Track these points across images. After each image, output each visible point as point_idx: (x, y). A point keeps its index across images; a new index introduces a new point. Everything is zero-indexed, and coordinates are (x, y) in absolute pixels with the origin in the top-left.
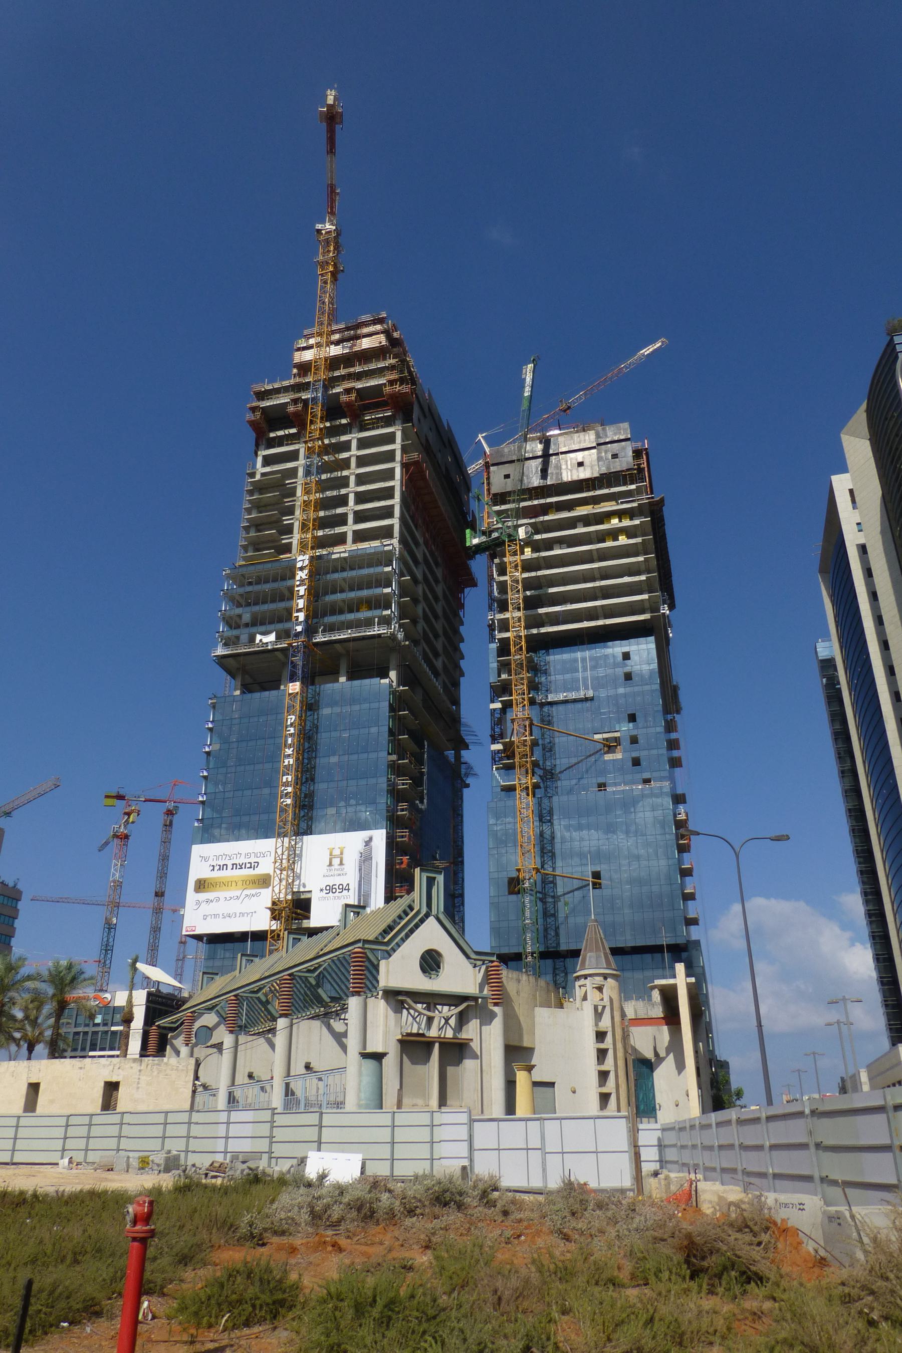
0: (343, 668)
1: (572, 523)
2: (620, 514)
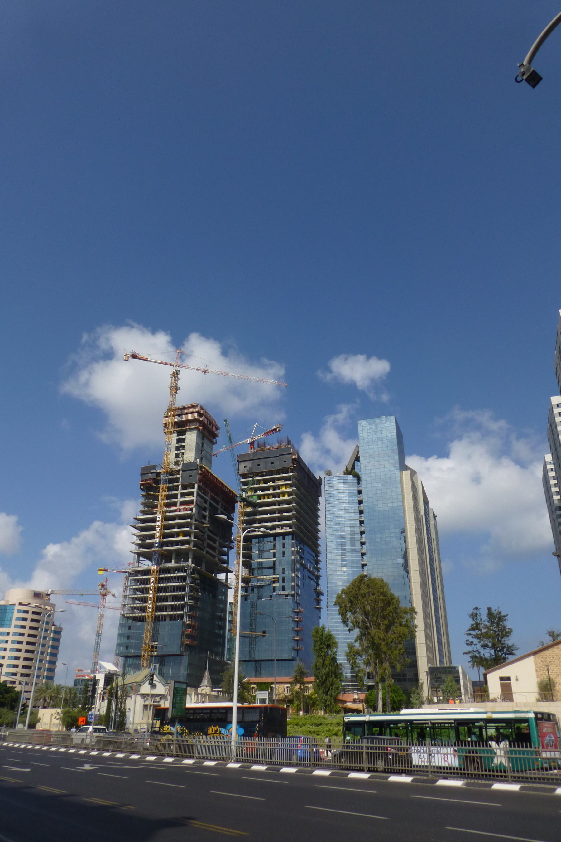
0: (173, 556)
1: (268, 489)
2: (286, 485)
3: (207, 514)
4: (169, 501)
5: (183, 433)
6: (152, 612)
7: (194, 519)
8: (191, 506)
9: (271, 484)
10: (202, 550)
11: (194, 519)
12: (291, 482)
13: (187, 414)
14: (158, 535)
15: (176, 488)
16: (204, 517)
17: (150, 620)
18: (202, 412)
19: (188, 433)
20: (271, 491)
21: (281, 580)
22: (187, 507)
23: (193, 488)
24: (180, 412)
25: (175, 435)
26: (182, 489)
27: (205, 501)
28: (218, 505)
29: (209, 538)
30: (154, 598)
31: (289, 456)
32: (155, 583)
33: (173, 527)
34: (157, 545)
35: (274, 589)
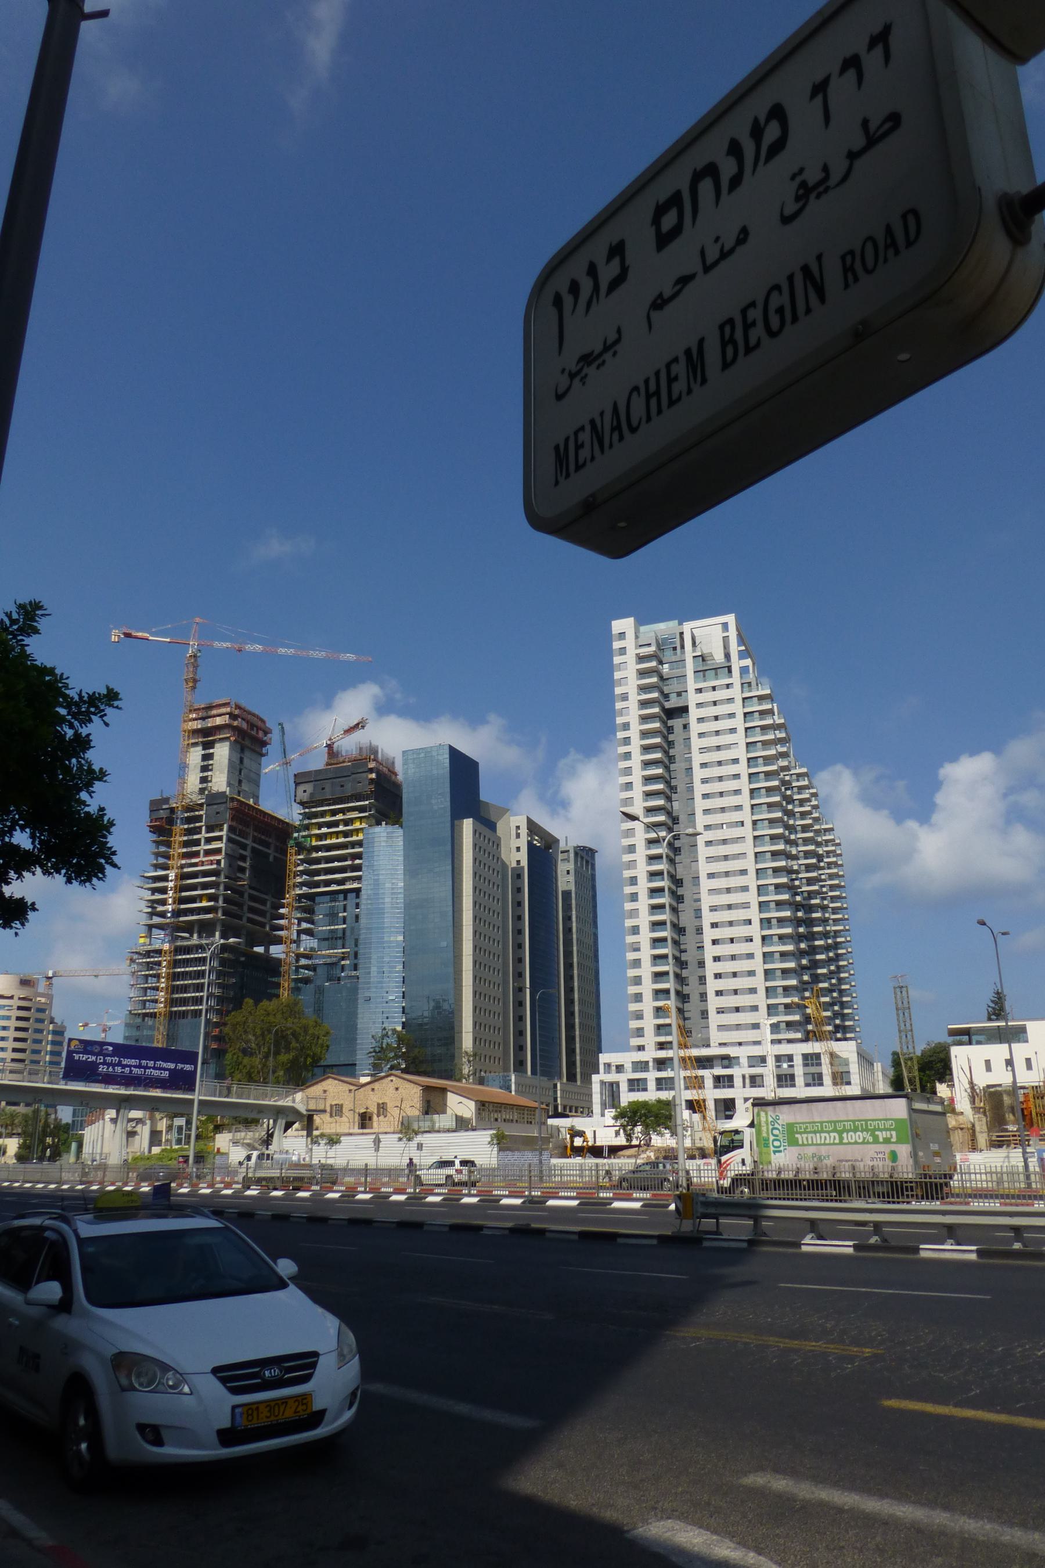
1: (336, 824)
3: (247, 865)
4: (189, 849)
5: (208, 745)
6: (165, 1007)
7: (222, 876)
8: (218, 857)
9: (340, 817)
10: (240, 918)
11: (222, 876)
12: (366, 814)
13: (214, 716)
14: (170, 901)
15: (198, 830)
16: (242, 870)
17: (162, 1018)
18: (237, 712)
19: (217, 745)
20: (341, 828)
21: (352, 955)
22: (212, 858)
23: (222, 830)
24: (205, 714)
25: (200, 748)
26: (207, 832)
27: (244, 847)
28: (268, 848)
29: (252, 898)
30: (167, 989)
31: (364, 775)
32: (168, 968)
33: (194, 887)
34: (169, 915)
35: (343, 968)
